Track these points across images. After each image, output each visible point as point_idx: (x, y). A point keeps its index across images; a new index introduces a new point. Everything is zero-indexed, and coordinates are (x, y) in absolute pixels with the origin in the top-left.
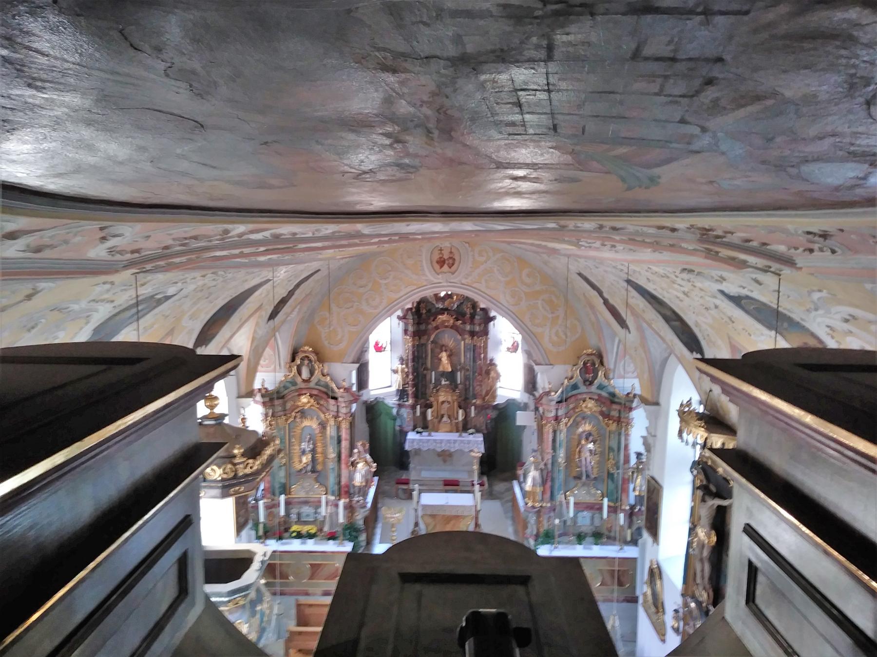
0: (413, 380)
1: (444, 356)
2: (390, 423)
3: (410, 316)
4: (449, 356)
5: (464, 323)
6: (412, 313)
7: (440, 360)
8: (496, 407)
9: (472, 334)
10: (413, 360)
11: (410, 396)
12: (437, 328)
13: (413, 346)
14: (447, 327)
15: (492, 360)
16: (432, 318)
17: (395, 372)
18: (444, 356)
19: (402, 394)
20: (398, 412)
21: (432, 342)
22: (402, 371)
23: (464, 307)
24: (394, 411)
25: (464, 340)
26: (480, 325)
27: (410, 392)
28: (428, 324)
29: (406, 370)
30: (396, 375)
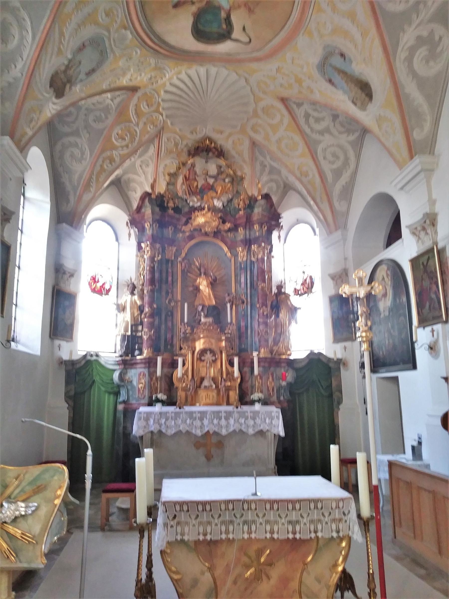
0: (152, 315)
1: (203, 285)
2: (108, 401)
3: (148, 211)
4: (213, 284)
5: (235, 229)
6: (151, 201)
7: (197, 289)
8: (291, 363)
9: (248, 243)
10: (152, 281)
11: (145, 345)
12: (191, 237)
13: (152, 259)
14: (206, 234)
15: (280, 287)
16: (184, 220)
17: (121, 308)
18: (203, 285)
19: (131, 343)
20: (121, 377)
21: (183, 259)
22: (133, 304)
23: (236, 201)
24: (116, 376)
25: (235, 256)
26: (261, 225)
27: (145, 337)
28: (177, 230)
29: (139, 303)
30: (121, 316)
